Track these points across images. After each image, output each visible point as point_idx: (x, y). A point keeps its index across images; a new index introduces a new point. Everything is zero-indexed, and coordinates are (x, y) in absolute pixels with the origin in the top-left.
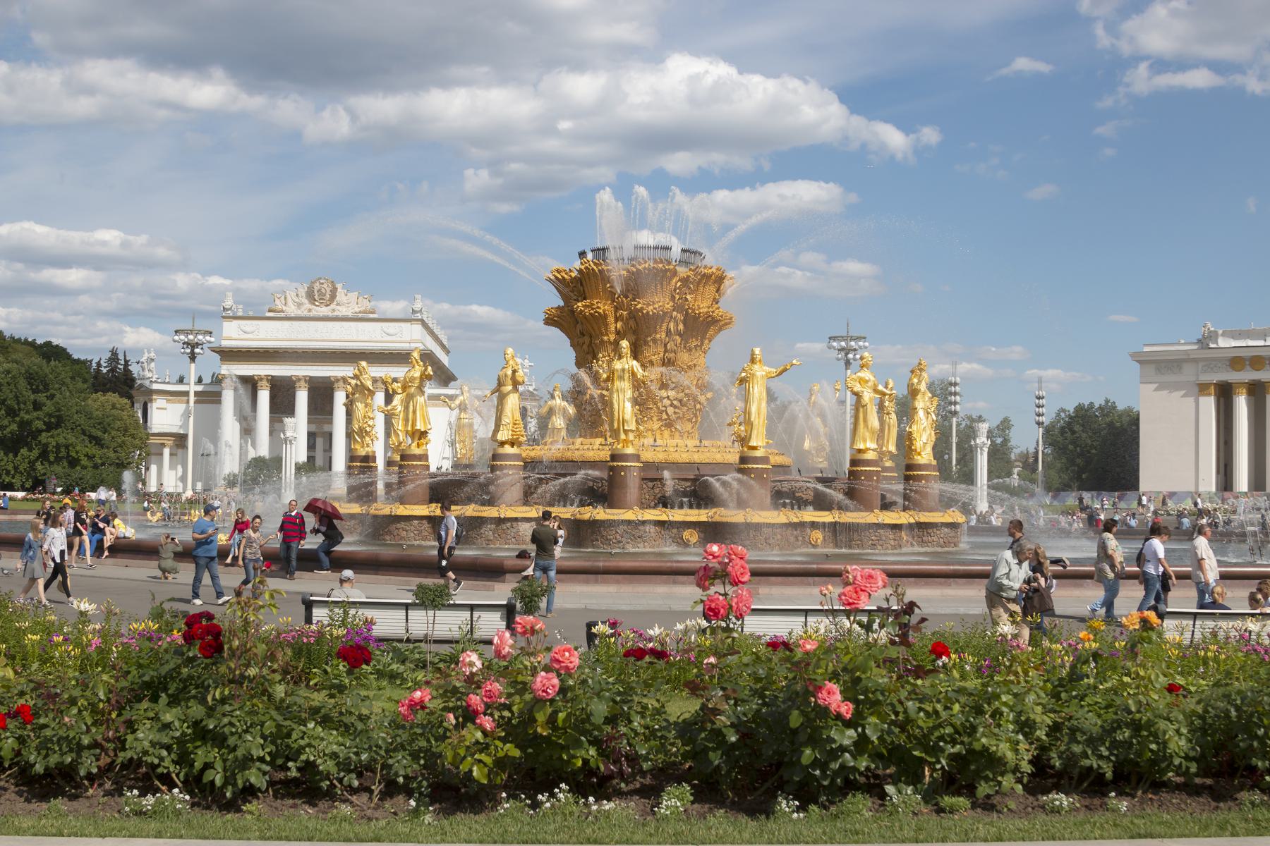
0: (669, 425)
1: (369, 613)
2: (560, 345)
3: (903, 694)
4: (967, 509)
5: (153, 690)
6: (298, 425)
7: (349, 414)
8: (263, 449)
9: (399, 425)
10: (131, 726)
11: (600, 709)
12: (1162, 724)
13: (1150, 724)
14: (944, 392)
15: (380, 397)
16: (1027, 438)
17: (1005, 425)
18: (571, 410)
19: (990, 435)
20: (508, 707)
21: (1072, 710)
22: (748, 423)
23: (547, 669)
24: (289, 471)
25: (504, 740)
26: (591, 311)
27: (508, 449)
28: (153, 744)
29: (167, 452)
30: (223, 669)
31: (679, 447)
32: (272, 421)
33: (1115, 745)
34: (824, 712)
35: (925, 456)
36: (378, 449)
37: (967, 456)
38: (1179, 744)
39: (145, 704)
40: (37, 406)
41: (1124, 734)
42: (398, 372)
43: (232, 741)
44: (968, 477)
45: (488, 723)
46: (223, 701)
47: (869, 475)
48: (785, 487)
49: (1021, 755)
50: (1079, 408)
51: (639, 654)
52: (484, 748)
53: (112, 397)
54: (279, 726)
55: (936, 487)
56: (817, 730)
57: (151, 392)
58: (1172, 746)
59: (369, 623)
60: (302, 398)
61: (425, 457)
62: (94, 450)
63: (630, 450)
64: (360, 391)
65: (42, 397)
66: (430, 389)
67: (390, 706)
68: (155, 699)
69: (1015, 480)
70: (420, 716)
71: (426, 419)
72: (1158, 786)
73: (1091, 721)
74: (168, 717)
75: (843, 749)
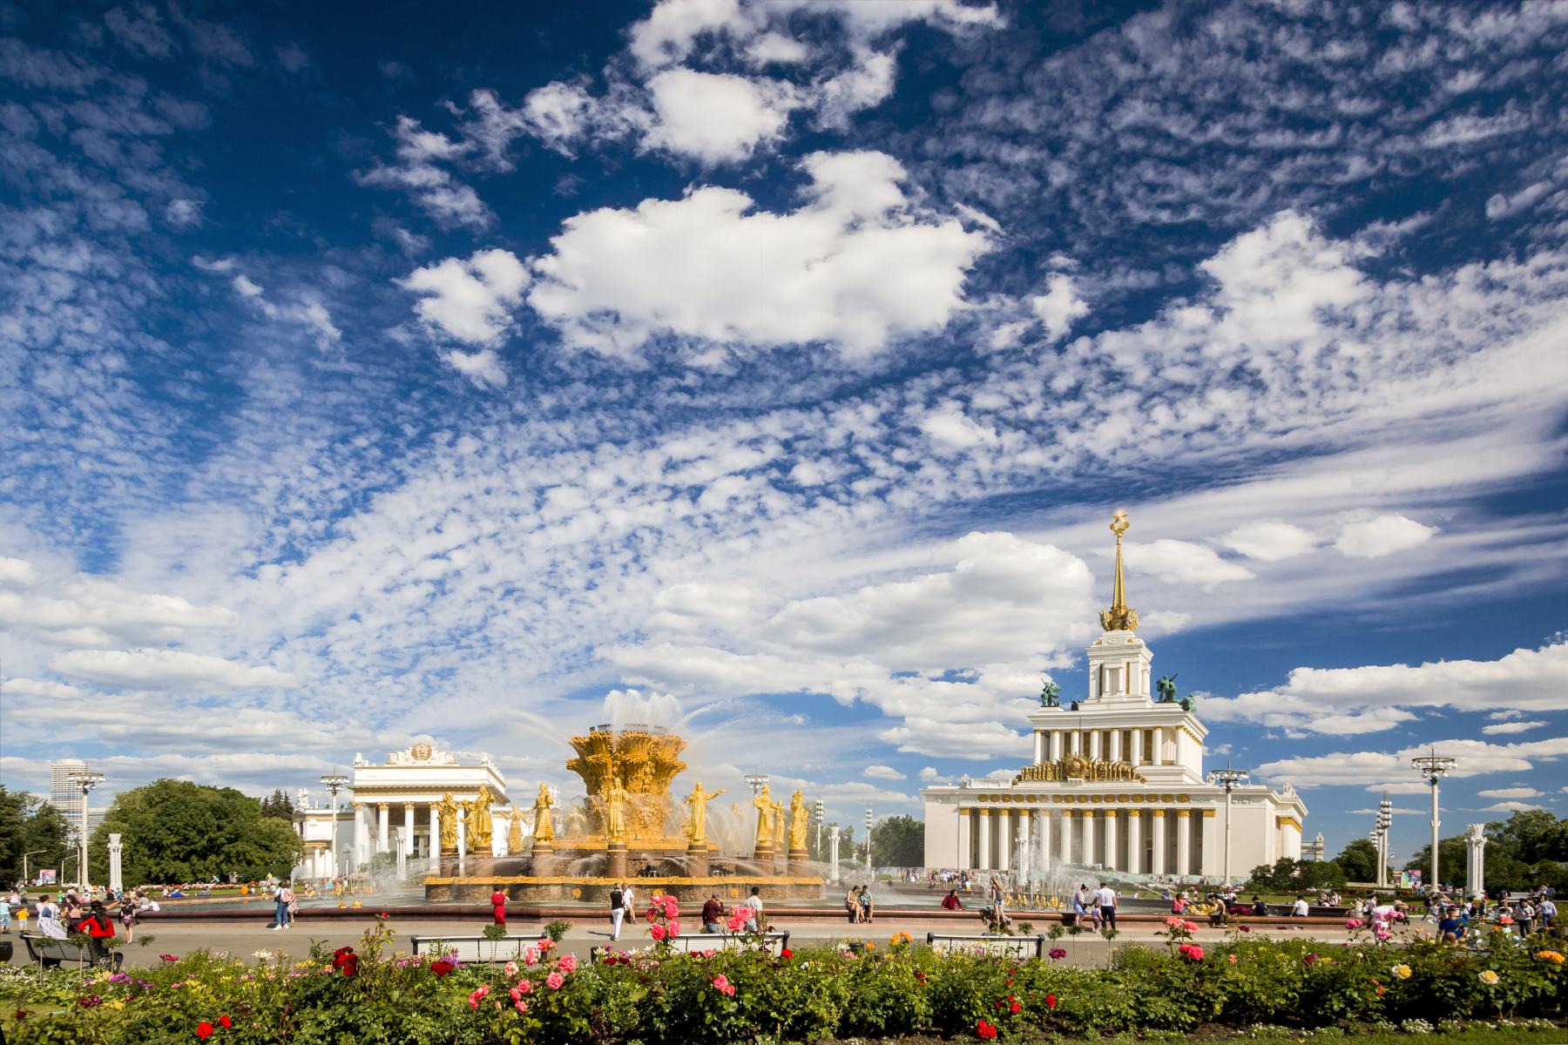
0: (646, 827)
1: (454, 945)
2: (578, 784)
3: (765, 980)
4: (826, 877)
5: (312, 1000)
6: (408, 830)
7: (441, 823)
8: (384, 845)
9: (473, 829)
10: (297, 1025)
11: (589, 996)
12: (911, 996)
13: (904, 997)
14: (813, 811)
15: (460, 814)
16: (863, 837)
17: (850, 831)
18: (584, 819)
19: (840, 834)
20: (534, 995)
21: (863, 989)
22: (694, 826)
23: (557, 970)
24: (401, 860)
25: (532, 1017)
26: (595, 762)
27: (543, 843)
28: (312, 1036)
29: (317, 852)
30: (358, 982)
31: (648, 841)
32: (390, 829)
33: (886, 1008)
34: (718, 992)
35: (800, 845)
36: (461, 845)
37: (826, 843)
38: (921, 1006)
39: (308, 1010)
40: (220, 828)
41: (890, 1002)
42: (472, 797)
43: (363, 1029)
44: (827, 859)
45: (523, 1006)
46: (358, 1003)
47: (767, 856)
48: (716, 863)
49: (829, 1013)
50: (891, 820)
51: (612, 961)
52: (521, 1024)
53: (276, 820)
54: (394, 1017)
55: (808, 864)
56: (715, 1003)
57: (305, 816)
58: (917, 1010)
59: (455, 952)
60: (410, 816)
61: (489, 848)
62: (266, 855)
63: (620, 843)
64: (448, 810)
65: (223, 823)
66: (493, 807)
67: (464, 999)
68: (314, 1006)
69: (854, 860)
70: (484, 1007)
71: (490, 826)
72: (910, 1033)
73: (874, 995)
74: (322, 1017)
75: (729, 1015)
